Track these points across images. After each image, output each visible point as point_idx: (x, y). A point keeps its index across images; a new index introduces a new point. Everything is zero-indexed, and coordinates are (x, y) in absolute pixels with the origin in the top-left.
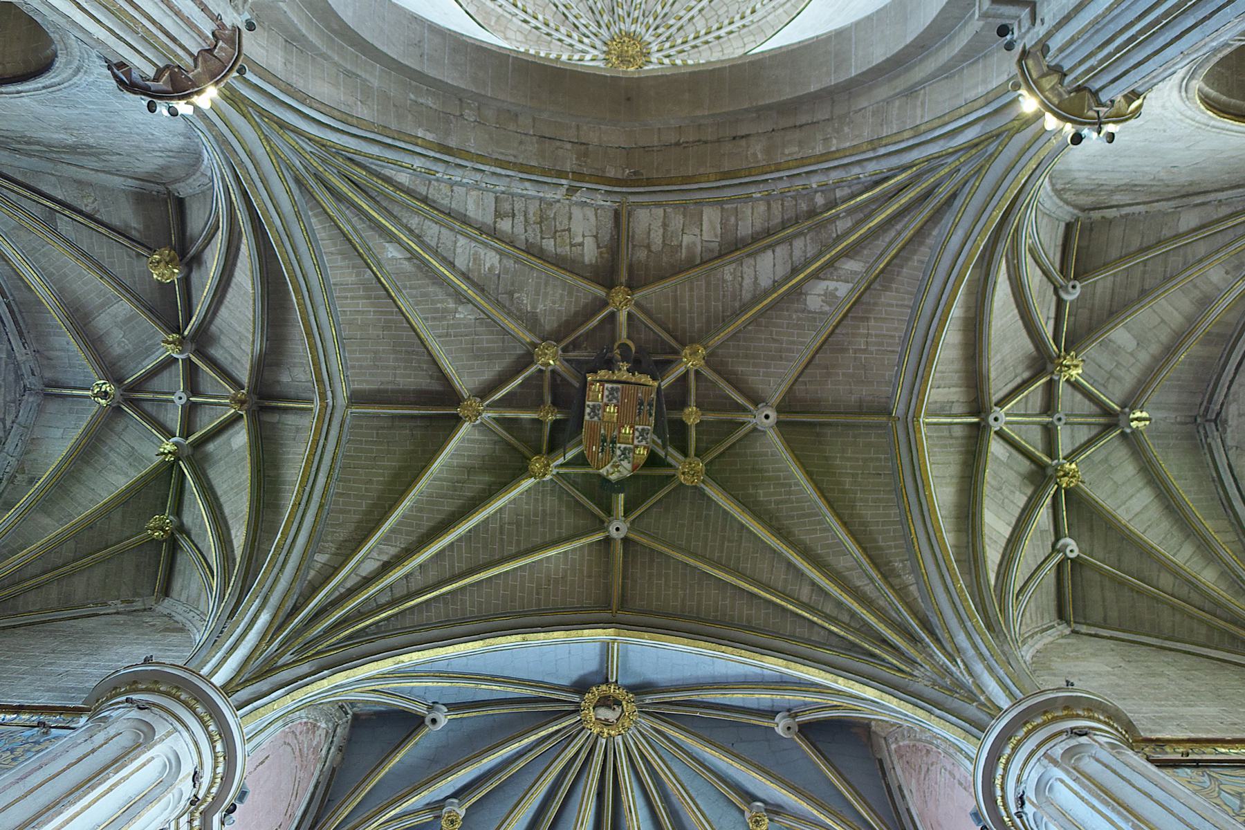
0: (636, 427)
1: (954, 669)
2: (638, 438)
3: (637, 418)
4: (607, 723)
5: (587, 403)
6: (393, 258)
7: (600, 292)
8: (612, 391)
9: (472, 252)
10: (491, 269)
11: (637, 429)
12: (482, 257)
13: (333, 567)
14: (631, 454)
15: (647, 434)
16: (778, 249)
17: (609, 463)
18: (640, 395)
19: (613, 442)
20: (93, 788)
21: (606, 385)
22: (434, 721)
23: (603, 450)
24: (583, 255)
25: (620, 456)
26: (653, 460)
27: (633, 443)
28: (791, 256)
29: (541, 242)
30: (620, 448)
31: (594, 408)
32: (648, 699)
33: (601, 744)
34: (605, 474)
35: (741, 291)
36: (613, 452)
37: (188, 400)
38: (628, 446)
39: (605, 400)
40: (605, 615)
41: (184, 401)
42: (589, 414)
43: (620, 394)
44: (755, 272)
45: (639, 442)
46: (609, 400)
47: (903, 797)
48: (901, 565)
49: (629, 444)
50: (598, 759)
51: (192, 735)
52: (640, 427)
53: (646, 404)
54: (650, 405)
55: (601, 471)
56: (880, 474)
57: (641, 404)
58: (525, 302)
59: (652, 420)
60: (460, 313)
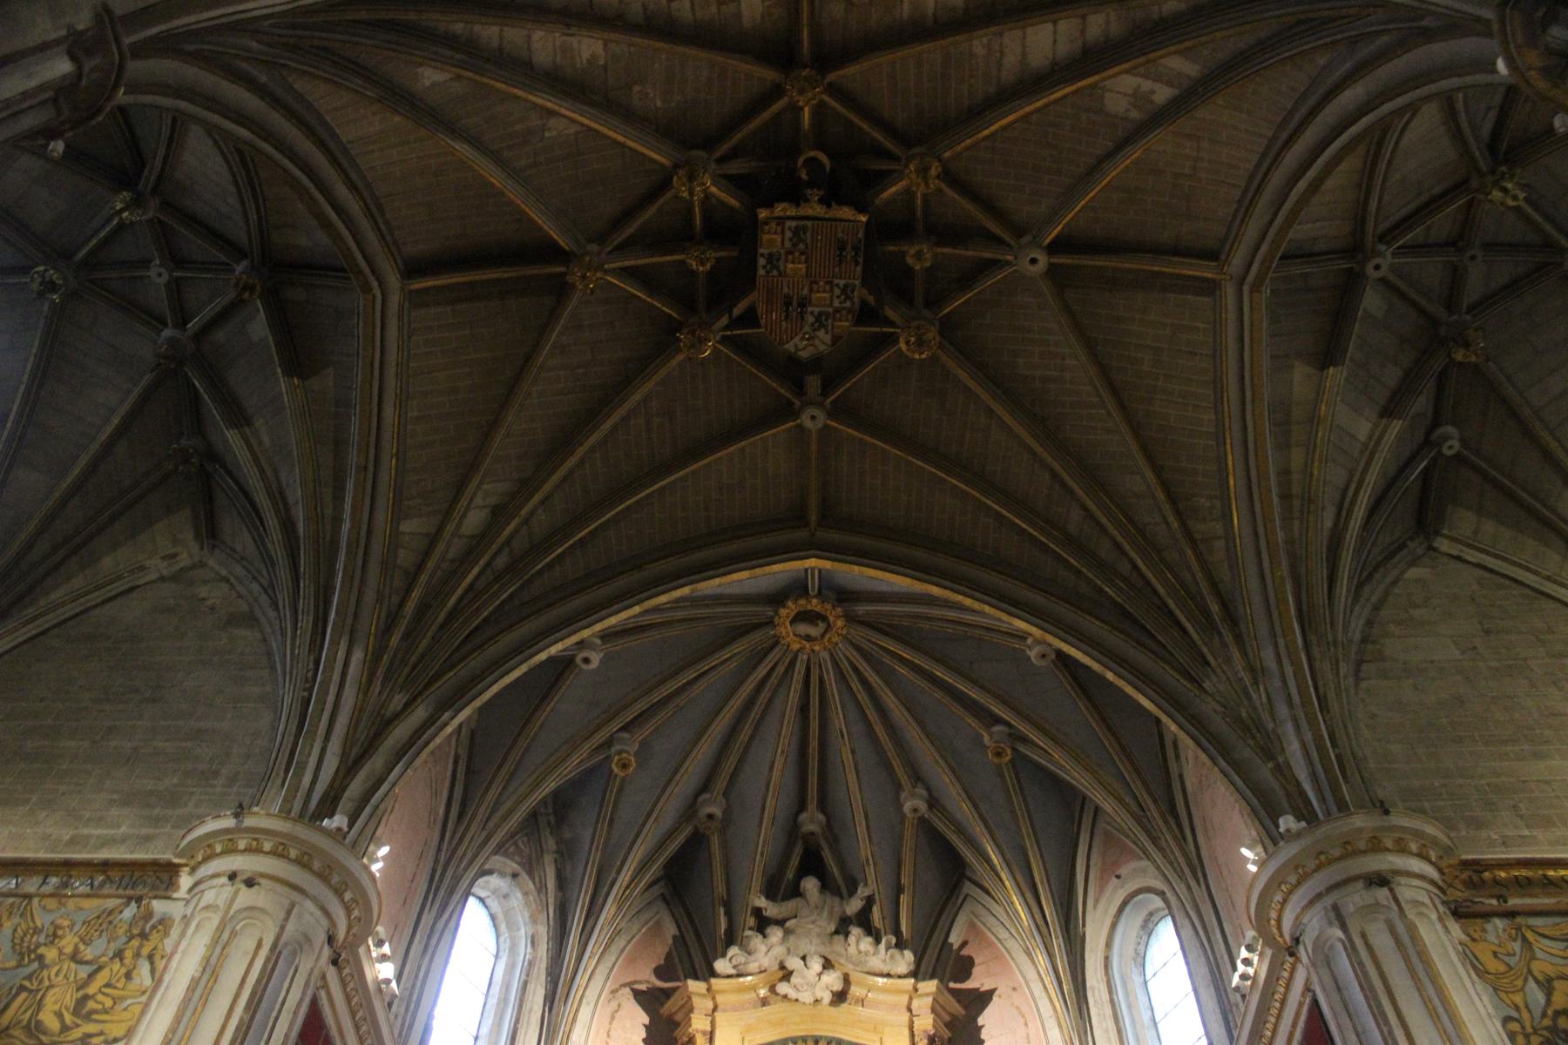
0: (836, 281)
1: (1254, 696)
2: (838, 297)
3: (837, 270)
4: (808, 638)
5: (761, 251)
6: (433, 85)
7: (770, 75)
8: (796, 231)
9: (558, 43)
10: (593, 57)
11: (838, 285)
12: (576, 46)
13: (427, 535)
14: (830, 321)
15: (853, 291)
16: (1063, 25)
17: (796, 335)
18: (840, 235)
19: (803, 304)
20: (238, 1029)
21: (788, 223)
22: (586, 660)
23: (786, 317)
24: (739, 15)
25: (813, 325)
26: (866, 314)
27: (831, 305)
28: (1083, 32)
29: (669, 7)
30: (812, 313)
31: (770, 258)
32: (862, 609)
33: (802, 660)
34: (793, 351)
35: (999, 70)
36: (803, 318)
37: (171, 276)
38: (826, 309)
39: (788, 245)
40: (800, 534)
41: (165, 278)
42: (764, 267)
43: (808, 235)
44: (1024, 47)
45: (841, 303)
46: (794, 245)
47: (1178, 757)
48: (1207, 504)
49: (825, 306)
50: (800, 668)
51: (314, 899)
52: (842, 282)
53: (849, 247)
54: (856, 249)
55: (786, 346)
56: (1196, 354)
57: (842, 248)
58: (651, 95)
59: (859, 269)
60: (550, 129)
